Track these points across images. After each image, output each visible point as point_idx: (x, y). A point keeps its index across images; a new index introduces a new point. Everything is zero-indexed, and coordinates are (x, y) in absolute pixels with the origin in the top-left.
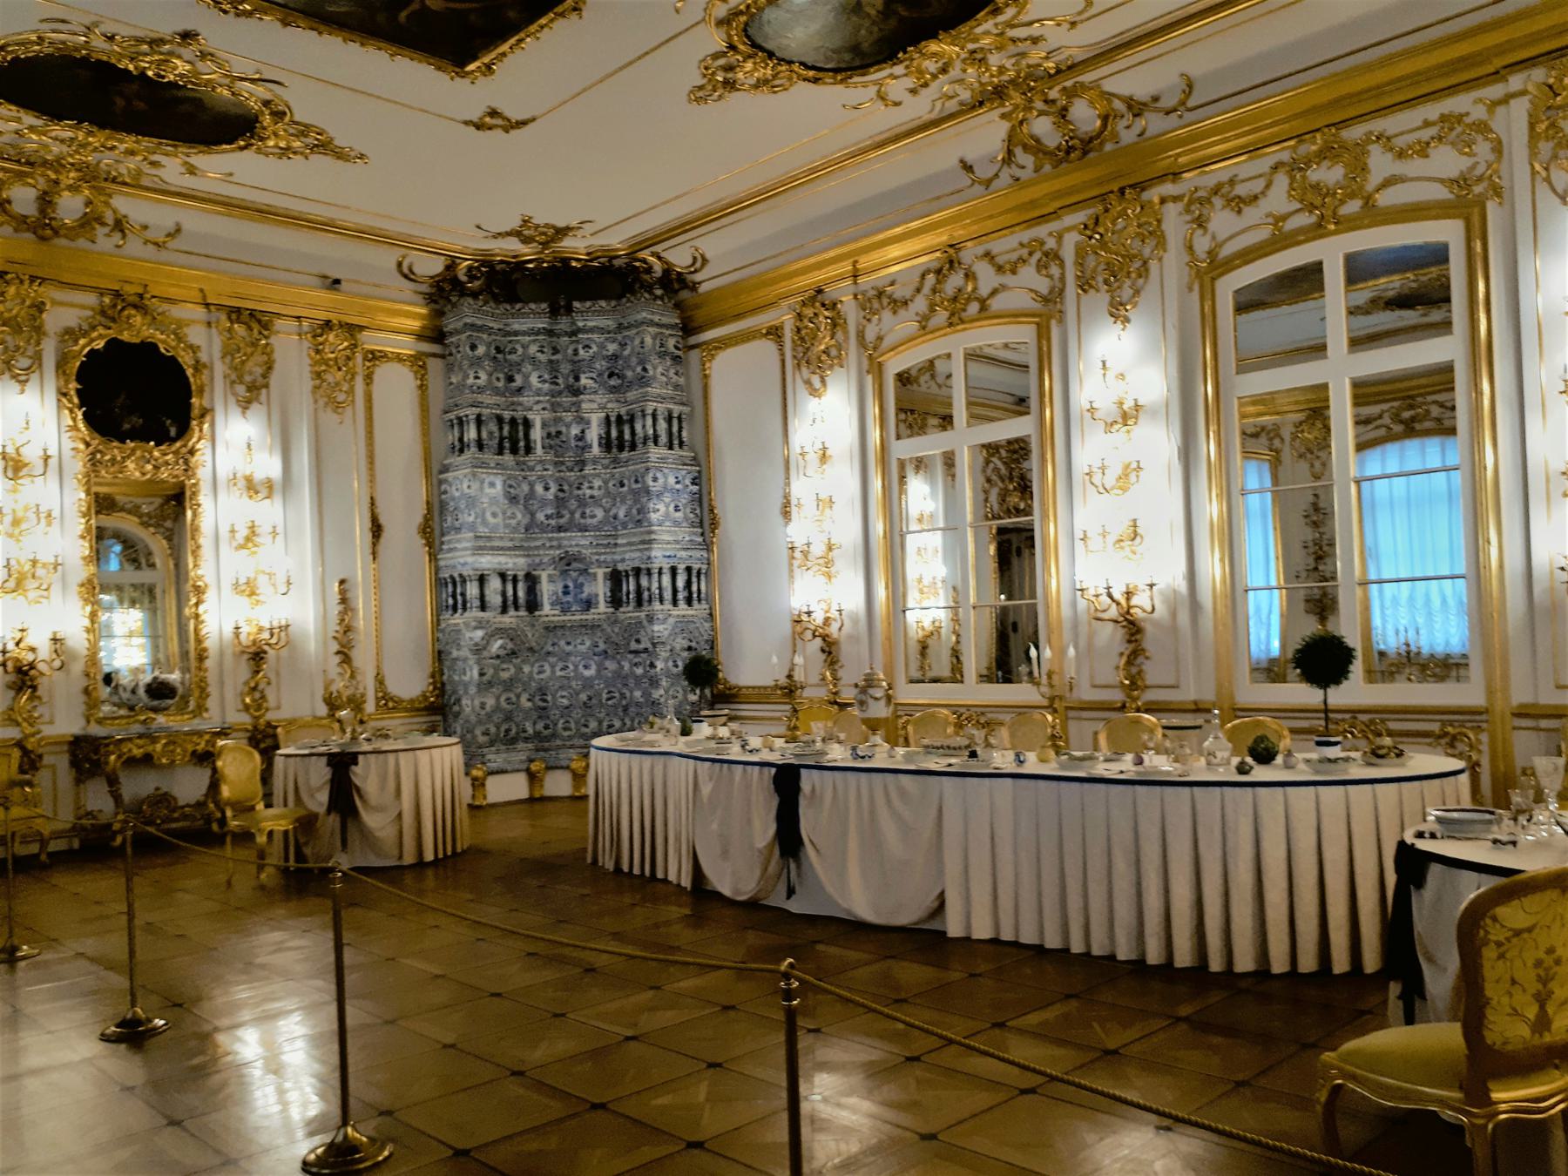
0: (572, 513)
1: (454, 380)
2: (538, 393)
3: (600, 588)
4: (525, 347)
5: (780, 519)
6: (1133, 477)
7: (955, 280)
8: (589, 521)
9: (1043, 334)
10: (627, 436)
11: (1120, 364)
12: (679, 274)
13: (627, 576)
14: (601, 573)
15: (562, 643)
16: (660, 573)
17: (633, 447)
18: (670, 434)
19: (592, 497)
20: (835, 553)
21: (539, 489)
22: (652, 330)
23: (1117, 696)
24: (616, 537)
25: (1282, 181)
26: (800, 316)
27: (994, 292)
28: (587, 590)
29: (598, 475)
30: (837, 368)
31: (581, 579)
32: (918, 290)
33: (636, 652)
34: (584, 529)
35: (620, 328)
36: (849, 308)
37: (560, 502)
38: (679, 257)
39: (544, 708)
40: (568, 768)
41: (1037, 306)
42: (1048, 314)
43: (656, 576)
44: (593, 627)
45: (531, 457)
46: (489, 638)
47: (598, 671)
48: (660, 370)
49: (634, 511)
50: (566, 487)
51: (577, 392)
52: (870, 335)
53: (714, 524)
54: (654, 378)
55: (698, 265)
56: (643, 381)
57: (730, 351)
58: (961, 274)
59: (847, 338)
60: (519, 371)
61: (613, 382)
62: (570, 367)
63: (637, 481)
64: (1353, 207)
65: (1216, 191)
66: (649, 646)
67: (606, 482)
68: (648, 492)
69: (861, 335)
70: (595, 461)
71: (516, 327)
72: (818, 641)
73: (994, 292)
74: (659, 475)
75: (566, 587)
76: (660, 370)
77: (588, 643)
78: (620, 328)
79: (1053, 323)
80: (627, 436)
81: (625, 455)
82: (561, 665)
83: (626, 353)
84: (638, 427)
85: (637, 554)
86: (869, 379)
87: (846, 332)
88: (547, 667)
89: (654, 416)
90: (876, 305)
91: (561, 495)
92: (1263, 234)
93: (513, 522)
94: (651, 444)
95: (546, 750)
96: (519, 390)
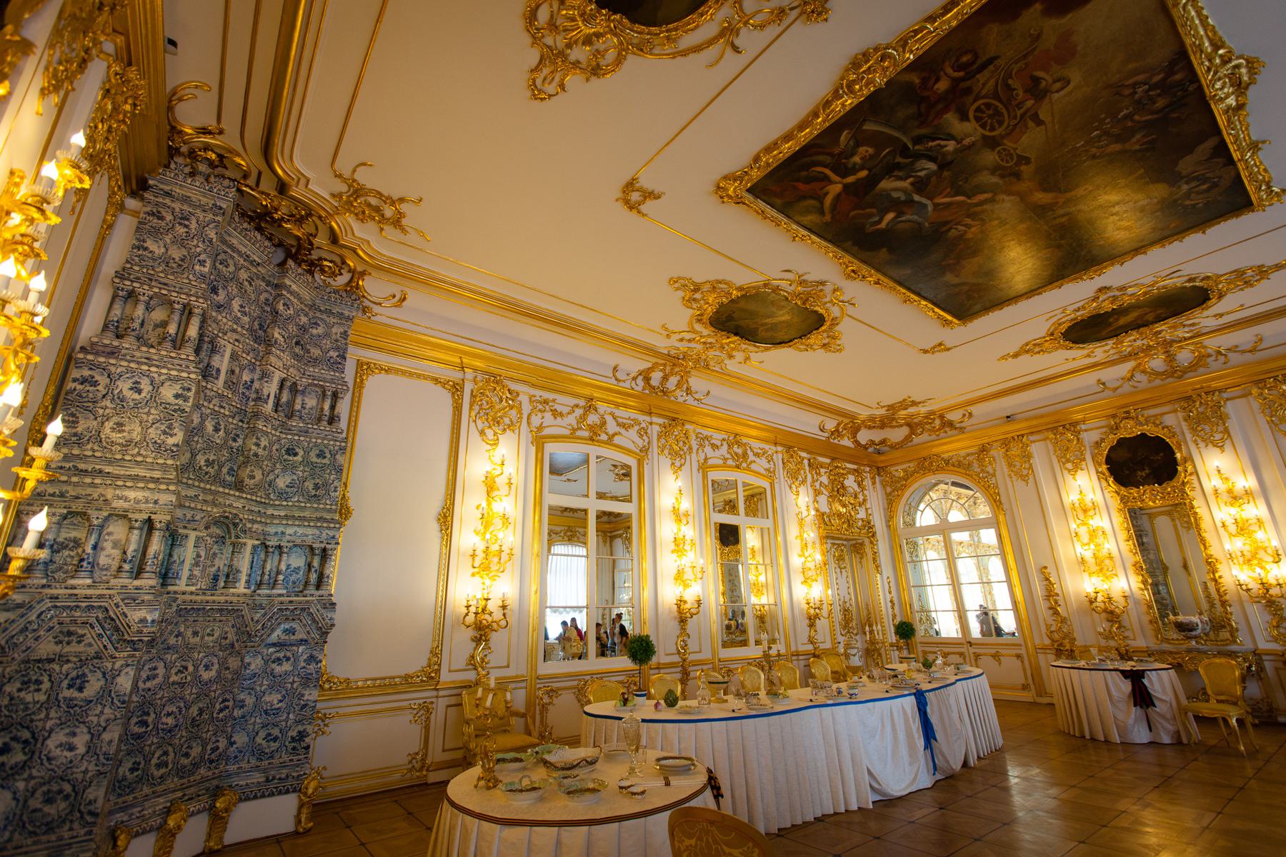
1: (155, 247)
2: (237, 320)
4: (238, 269)
7: (593, 419)
10: (298, 407)
14: (250, 543)
15: (189, 633)
19: (256, 455)
21: (209, 427)
23: (676, 659)
25: (725, 446)
29: (266, 433)
35: (313, 307)
38: (373, 287)
39: (139, 737)
47: (219, 672)
49: (309, 485)
51: (269, 343)
53: (345, 512)
60: (225, 287)
61: (297, 350)
64: (744, 465)
65: (707, 438)
67: (271, 444)
71: (235, 241)
77: (217, 634)
83: (314, 331)
86: (533, 449)
88: (161, 671)
92: (721, 462)
96: (219, 307)
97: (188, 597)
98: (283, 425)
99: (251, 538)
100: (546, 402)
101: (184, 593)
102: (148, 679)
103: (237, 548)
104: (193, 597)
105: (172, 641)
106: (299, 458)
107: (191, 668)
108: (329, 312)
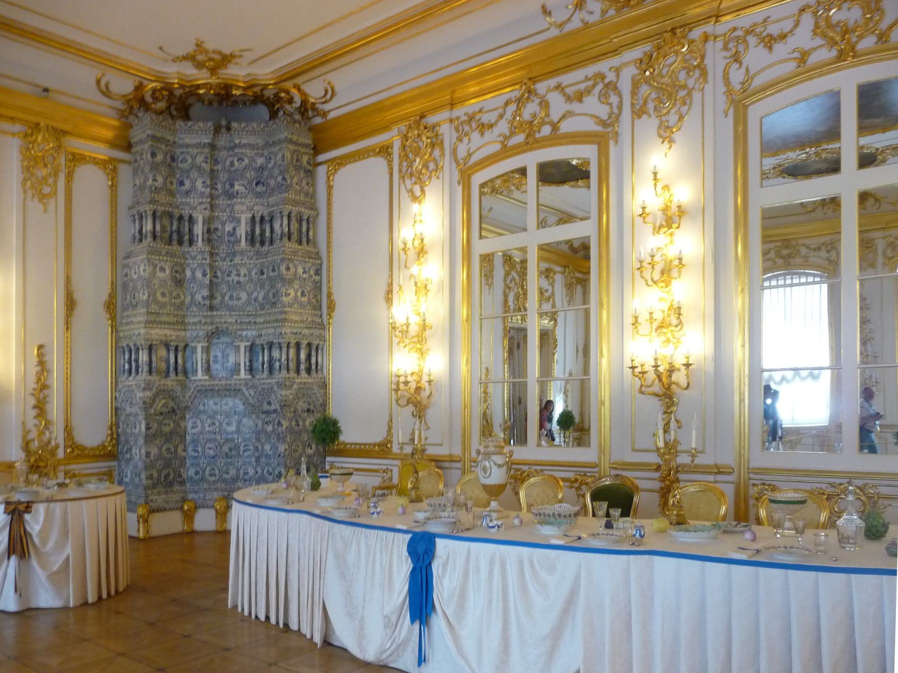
0: (223, 296)
3: (243, 359)
5: (383, 304)
6: (674, 273)
7: (531, 108)
8: (235, 302)
9: (603, 154)
10: (268, 234)
11: (663, 179)
12: (313, 104)
13: (263, 349)
14: (242, 346)
15: (211, 402)
16: (288, 347)
17: (272, 242)
18: (300, 230)
19: (239, 282)
20: (427, 333)
22: (292, 147)
24: (255, 316)
26: (405, 137)
27: (564, 117)
28: (232, 359)
30: (434, 179)
31: (227, 351)
32: (501, 116)
33: (267, 413)
34: (231, 309)
35: (267, 145)
36: (446, 130)
37: (212, 285)
39: (195, 458)
40: (212, 507)
41: (599, 128)
42: (603, 136)
43: (285, 349)
44: (235, 390)
45: (194, 248)
46: (153, 400)
48: (295, 180)
49: (271, 295)
50: (219, 274)
52: (462, 152)
54: (291, 185)
55: (328, 96)
56: (283, 187)
57: (349, 167)
58: (537, 101)
59: (443, 155)
61: (259, 189)
62: (226, 175)
63: (273, 270)
66: (278, 407)
67: (250, 271)
68: (283, 280)
69: (454, 152)
70: (242, 253)
72: (411, 408)
73: (564, 117)
74: (291, 265)
75: (216, 357)
76: (295, 180)
78: (267, 145)
79: (611, 142)
80: (268, 234)
81: (265, 248)
82: (209, 421)
83: (270, 166)
84: (277, 226)
85: (271, 331)
87: (442, 150)
88: (199, 424)
89: (289, 217)
90: (467, 128)
91: (215, 280)
93: (178, 301)
94: (285, 239)
95: (196, 493)
97: (200, 383)
98: (257, 253)
99: (242, 341)
100: (471, 118)
101: (200, 380)
102: (193, 428)
103: (238, 348)
104: (203, 383)
105: (201, 408)
106: (265, 276)
107: (217, 424)
108: (274, 143)
